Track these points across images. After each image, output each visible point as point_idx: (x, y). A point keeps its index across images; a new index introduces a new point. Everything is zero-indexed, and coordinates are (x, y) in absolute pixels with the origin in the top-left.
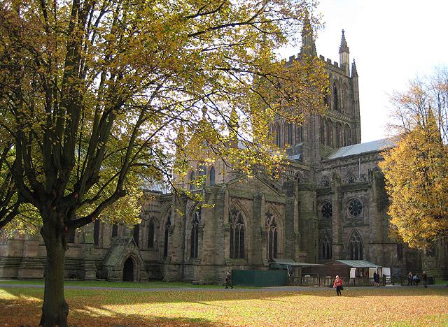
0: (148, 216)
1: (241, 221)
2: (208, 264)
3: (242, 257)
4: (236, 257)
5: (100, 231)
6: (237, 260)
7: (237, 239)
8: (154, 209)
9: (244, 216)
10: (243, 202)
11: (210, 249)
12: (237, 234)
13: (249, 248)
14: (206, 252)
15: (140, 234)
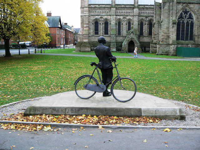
0: (148, 19)
1: (191, 17)
2: (165, 43)
3: (190, 39)
4: (187, 39)
5: (121, 28)
6: (187, 42)
7: (187, 29)
8: (151, 15)
9: (193, 15)
10: (192, 6)
11: (165, 35)
12: (188, 25)
13: (196, 34)
14: (163, 37)
15: (144, 29)
